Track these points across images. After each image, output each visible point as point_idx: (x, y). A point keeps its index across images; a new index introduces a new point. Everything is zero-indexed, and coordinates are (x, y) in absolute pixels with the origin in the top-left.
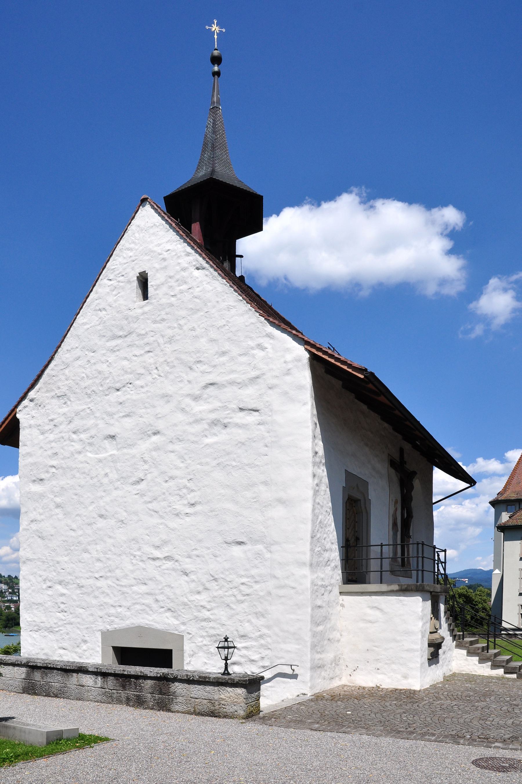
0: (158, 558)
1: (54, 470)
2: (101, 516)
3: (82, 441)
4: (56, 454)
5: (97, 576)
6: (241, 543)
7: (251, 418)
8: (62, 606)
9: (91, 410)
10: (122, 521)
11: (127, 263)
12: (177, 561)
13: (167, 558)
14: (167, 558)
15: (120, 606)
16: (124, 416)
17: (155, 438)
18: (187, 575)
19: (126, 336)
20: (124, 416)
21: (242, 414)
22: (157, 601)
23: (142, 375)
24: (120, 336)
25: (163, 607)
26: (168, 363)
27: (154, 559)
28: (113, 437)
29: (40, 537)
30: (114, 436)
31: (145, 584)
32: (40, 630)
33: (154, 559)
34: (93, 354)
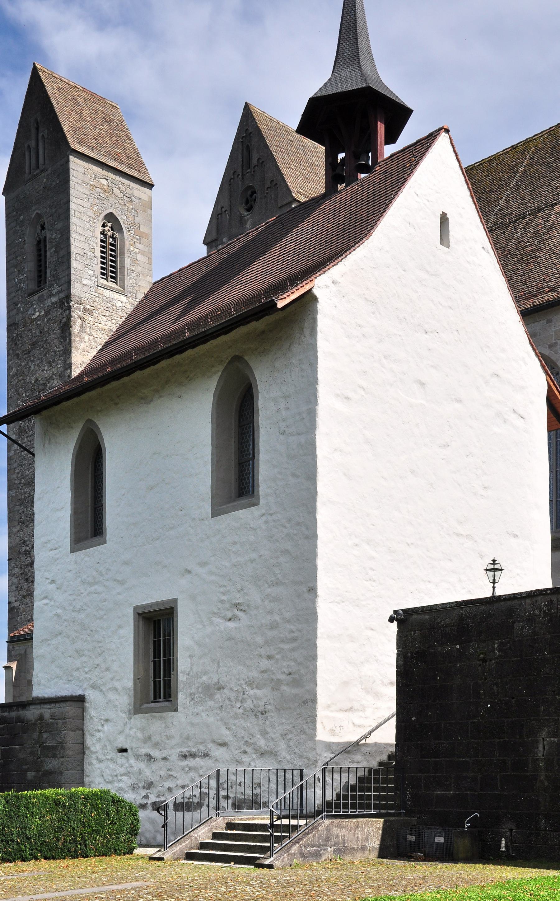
0: (462, 535)
1: (362, 392)
2: (412, 472)
3: (393, 371)
4: (365, 373)
5: (409, 543)
6: (516, 536)
7: (519, 423)
8: (371, 572)
9: (402, 339)
10: (431, 484)
11: (432, 189)
12: (476, 541)
13: (468, 536)
14: (468, 536)
15: (429, 582)
16: (432, 366)
17: (457, 405)
18: (481, 558)
19: (432, 275)
20: (432, 366)
21: (514, 416)
22: (460, 581)
23: (446, 329)
24: (427, 271)
25: (464, 588)
26: (466, 332)
27: (458, 535)
28: (422, 384)
29: (345, 474)
30: (424, 384)
31: (451, 560)
32: (343, 602)
33: (458, 535)
34: (403, 272)
